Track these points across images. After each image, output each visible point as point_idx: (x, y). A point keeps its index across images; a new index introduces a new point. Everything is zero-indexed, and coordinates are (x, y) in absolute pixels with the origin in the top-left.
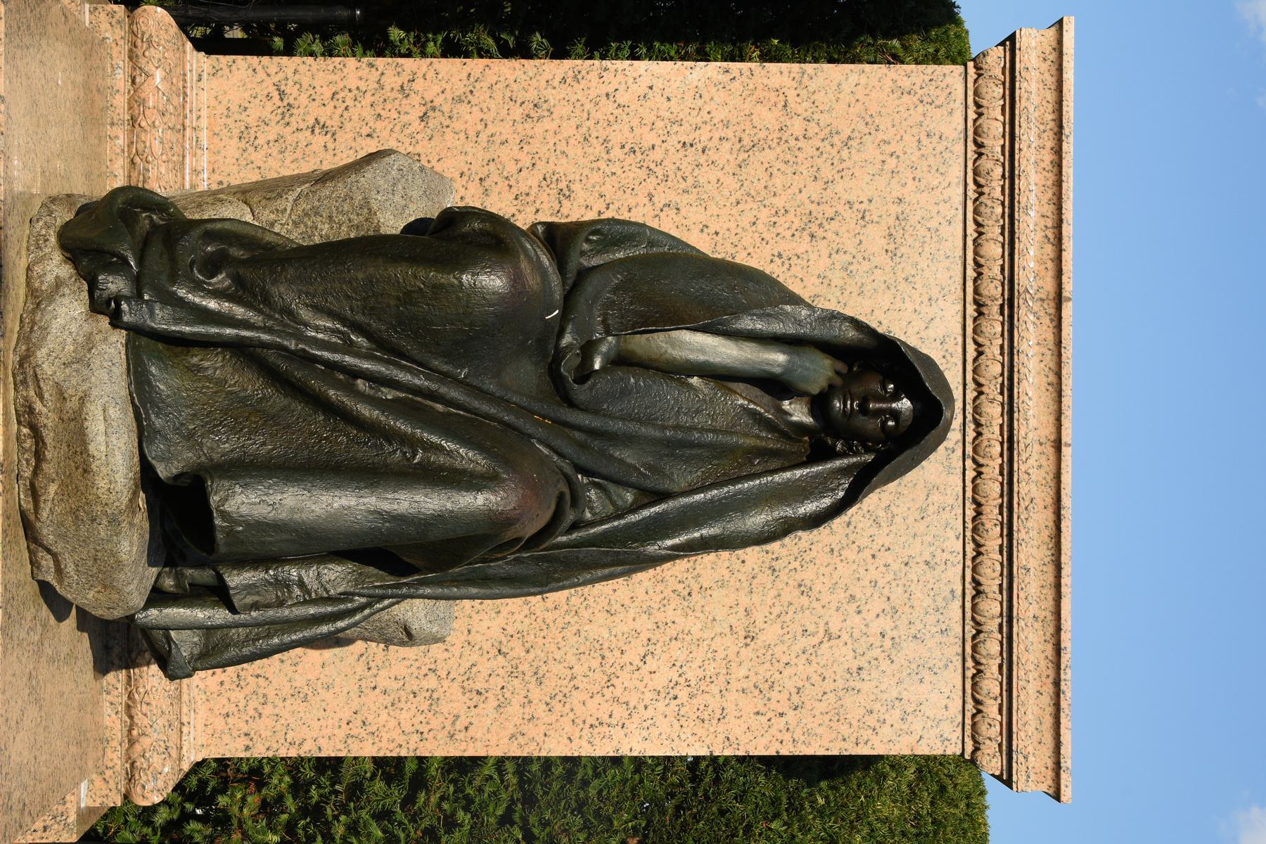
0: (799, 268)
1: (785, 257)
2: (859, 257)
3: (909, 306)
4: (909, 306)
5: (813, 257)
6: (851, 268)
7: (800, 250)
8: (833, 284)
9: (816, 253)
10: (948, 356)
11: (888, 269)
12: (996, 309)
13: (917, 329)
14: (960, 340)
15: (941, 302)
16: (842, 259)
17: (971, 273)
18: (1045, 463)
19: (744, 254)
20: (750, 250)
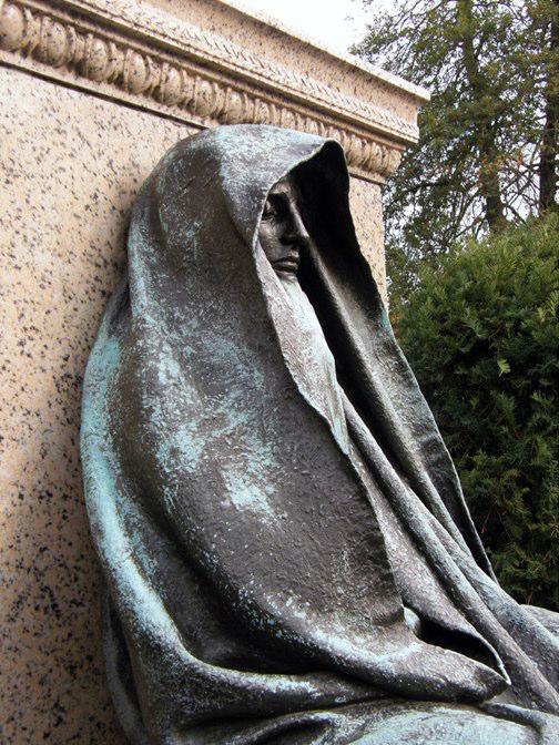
0: (35, 315)
1: (22, 336)
2: (17, 225)
3: (66, 163)
4: (66, 163)
5: (20, 294)
6: (30, 238)
7: (13, 312)
8: (50, 268)
9: (18, 289)
10: (115, 122)
11: (28, 184)
12: (79, 42)
13: (90, 158)
14: (98, 102)
15: (62, 116)
16: (21, 250)
17: (28, 64)
18: (228, 31)
19: (23, 395)
20: (17, 387)
